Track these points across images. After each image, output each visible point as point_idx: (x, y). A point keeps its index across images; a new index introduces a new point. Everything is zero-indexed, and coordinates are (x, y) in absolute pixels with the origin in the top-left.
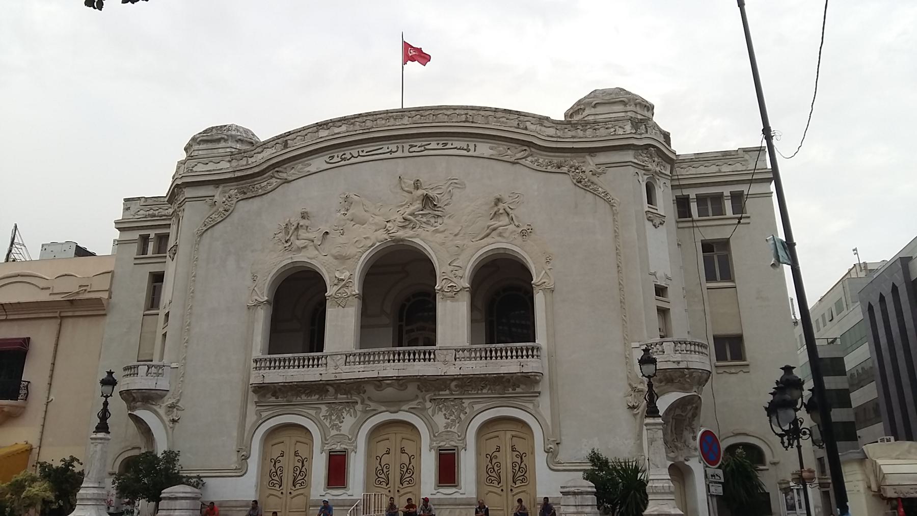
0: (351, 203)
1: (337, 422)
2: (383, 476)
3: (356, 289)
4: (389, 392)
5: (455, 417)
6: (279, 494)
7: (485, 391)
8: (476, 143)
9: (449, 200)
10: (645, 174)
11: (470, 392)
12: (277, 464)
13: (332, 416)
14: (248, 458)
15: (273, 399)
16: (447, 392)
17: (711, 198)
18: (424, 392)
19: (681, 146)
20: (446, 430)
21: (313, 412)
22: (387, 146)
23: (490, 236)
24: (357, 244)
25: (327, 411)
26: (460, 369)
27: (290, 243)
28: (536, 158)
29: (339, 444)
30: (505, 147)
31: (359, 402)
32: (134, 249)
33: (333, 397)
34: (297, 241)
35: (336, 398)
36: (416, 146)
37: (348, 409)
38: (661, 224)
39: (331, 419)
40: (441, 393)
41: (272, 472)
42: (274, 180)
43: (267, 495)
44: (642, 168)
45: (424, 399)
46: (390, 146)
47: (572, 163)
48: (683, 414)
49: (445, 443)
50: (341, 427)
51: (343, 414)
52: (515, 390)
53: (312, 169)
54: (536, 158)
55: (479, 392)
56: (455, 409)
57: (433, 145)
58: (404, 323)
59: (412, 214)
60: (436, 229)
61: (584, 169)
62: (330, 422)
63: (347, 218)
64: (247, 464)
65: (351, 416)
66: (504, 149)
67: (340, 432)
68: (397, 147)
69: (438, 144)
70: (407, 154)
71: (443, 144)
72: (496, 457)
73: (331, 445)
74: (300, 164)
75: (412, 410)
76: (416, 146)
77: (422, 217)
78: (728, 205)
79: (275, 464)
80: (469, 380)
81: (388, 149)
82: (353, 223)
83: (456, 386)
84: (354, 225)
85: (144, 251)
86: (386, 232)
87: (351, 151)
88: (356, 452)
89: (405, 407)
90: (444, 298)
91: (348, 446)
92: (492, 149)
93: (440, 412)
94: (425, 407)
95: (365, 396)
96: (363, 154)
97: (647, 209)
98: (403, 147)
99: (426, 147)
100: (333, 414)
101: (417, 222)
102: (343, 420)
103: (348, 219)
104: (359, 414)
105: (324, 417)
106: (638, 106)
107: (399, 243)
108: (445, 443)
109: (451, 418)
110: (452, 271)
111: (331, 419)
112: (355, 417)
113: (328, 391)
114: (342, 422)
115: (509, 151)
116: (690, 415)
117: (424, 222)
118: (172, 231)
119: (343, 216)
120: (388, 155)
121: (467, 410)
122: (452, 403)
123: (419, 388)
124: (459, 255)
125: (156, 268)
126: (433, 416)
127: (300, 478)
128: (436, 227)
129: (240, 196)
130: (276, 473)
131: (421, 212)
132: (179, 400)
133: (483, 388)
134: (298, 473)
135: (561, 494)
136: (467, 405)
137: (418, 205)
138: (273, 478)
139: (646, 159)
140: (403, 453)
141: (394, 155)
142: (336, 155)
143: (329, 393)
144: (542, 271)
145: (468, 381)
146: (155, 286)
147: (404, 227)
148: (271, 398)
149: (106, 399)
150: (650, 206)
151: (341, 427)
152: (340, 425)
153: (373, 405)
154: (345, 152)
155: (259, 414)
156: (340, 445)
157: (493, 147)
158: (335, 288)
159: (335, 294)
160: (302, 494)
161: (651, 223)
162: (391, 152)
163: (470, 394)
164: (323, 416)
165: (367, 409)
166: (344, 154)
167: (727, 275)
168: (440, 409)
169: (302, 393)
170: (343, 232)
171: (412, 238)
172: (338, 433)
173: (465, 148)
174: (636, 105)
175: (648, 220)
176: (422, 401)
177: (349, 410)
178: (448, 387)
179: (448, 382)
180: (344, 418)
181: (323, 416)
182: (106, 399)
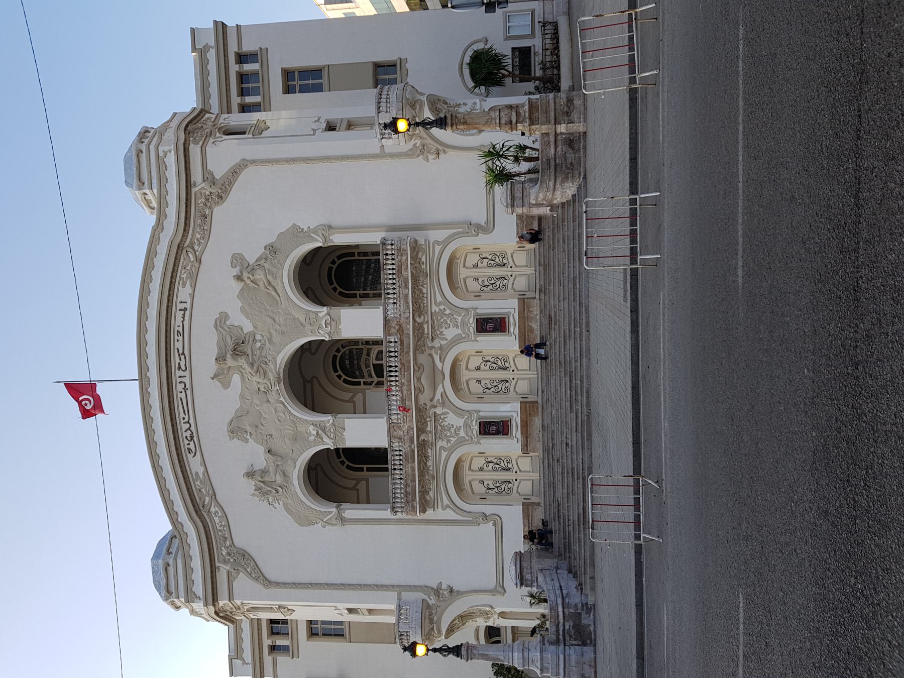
0: (239, 428)
1: (452, 430)
2: (500, 386)
3: (328, 419)
4: (423, 381)
6: (516, 483)
7: (424, 291)
8: (179, 301)
9: (238, 329)
10: (215, 135)
11: (425, 305)
12: (490, 487)
14: (485, 514)
15: (431, 493)
16: (425, 326)
17: (242, 83)
18: (426, 348)
19: (188, 102)
21: (444, 454)
22: (179, 393)
23: (276, 288)
24: (282, 421)
25: (443, 440)
27: (279, 488)
28: (196, 241)
29: (472, 427)
30: (183, 271)
31: (433, 410)
32: (282, 659)
34: (277, 482)
35: (431, 432)
36: (179, 363)
38: (265, 123)
39: (450, 437)
40: (426, 332)
41: (497, 491)
42: (213, 509)
43: (518, 495)
44: (208, 138)
45: (433, 347)
46: (179, 391)
47: (202, 205)
48: (444, 111)
49: (471, 328)
53: (201, 470)
54: (196, 241)
55: (425, 296)
56: (440, 319)
57: (179, 345)
58: (362, 380)
59: (252, 365)
60: (268, 339)
61: (207, 193)
62: (453, 437)
63: (254, 431)
64: (490, 515)
66: (185, 272)
68: (180, 382)
69: (178, 341)
70: (187, 373)
71: (178, 335)
72: (483, 281)
73: (474, 435)
74: (196, 483)
75: (442, 360)
76: (179, 363)
77: (255, 355)
78: (248, 67)
79: (490, 489)
80: (415, 305)
81: (181, 392)
82: (260, 426)
83: (420, 317)
84: (262, 424)
85: (284, 649)
86: (270, 392)
87: (184, 430)
88: (480, 411)
89: (439, 365)
90: (338, 331)
92: (185, 285)
93: (444, 333)
94: (438, 347)
95: (429, 404)
96: (187, 417)
97: (251, 136)
98: (180, 377)
99: (180, 353)
100: (446, 435)
101: (261, 359)
103: (256, 431)
104: (445, 410)
106: (143, 140)
107: (282, 378)
108: (471, 328)
109: (449, 322)
110: (311, 324)
112: (448, 413)
113: (424, 440)
114: (453, 425)
115: (188, 268)
116: (445, 106)
117: (261, 353)
118: (265, 616)
119: (252, 437)
120: (188, 392)
121: (442, 307)
122: (436, 322)
123: (423, 353)
124: (294, 318)
125: (303, 631)
126: (447, 340)
127: (502, 464)
128: (265, 341)
129: (228, 543)
130: (498, 487)
131: (250, 357)
132: (432, 588)
133: (421, 291)
134: (498, 466)
135: (515, 214)
136: (438, 308)
137: (242, 361)
138: (503, 490)
139: (199, 133)
141: (188, 386)
142: (187, 446)
143: (426, 439)
144: (311, 236)
145: (415, 305)
146: (324, 635)
147: (265, 374)
148: (430, 496)
149: (430, 650)
150: (247, 133)
153: (438, 396)
154: (184, 436)
155: (444, 508)
157: (183, 284)
158: (326, 439)
159: (332, 439)
160: (517, 461)
161: (265, 134)
162: (185, 389)
163: (427, 306)
165: (441, 402)
166: (186, 437)
167: (317, 72)
168: (441, 333)
170: (269, 435)
171: (276, 365)
172: (462, 428)
173: (183, 312)
174: (142, 142)
175: (261, 134)
176: (433, 350)
178: (421, 325)
179: (416, 325)
182: (430, 650)
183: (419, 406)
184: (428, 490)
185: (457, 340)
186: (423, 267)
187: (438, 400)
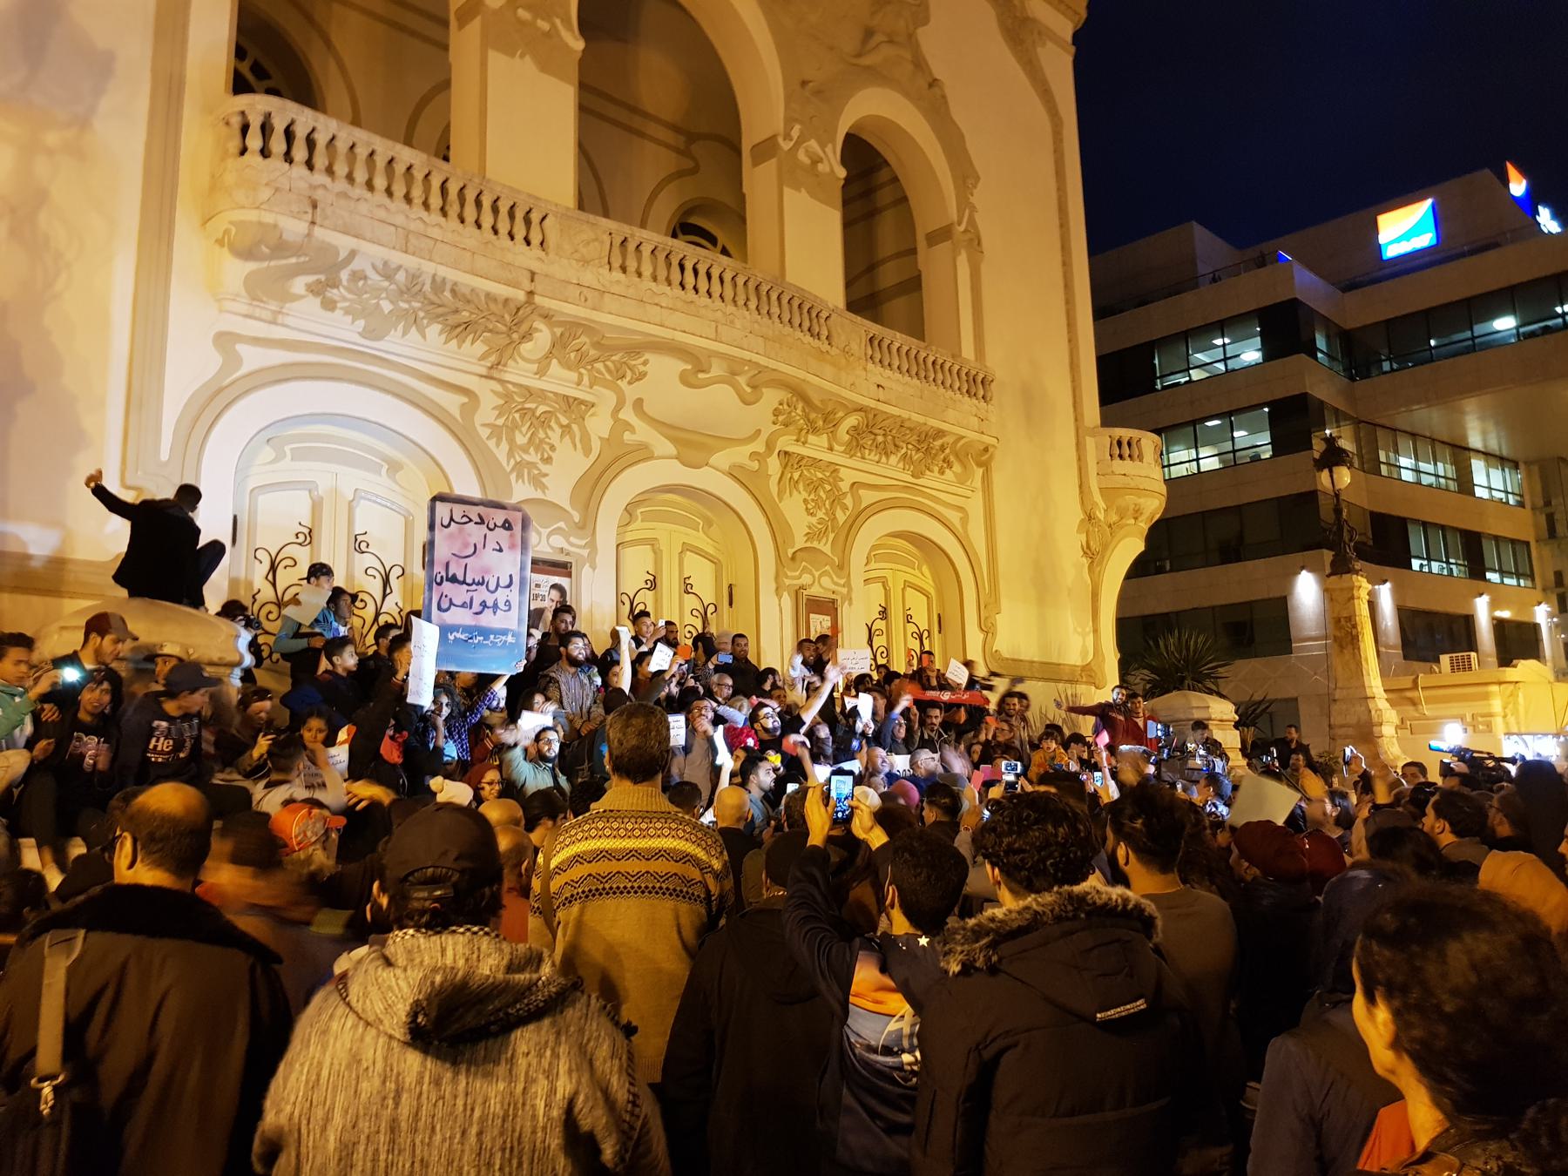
1: (532, 457)
5: (826, 514)
7: (894, 459)
12: (280, 571)
13: (517, 432)
16: (823, 440)
20: (808, 545)
25: (501, 412)
26: (878, 386)
33: (535, 367)
37: (564, 421)
39: (511, 441)
40: (812, 438)
50: (546, 475)
51: (550, 433)
52: (942, 472)
62: (510, 454)
65: (575, 446)
67: (544, 492)
91: (572, 545)
95: (631, 392)
102: (553, 455)
104: (596, 446)
105: (488, 431)
109: (821, 514)
111: (511, 441)
114: (548, 460)
121: (848, 501)
140: (689, 593)
148: (300, 297)
151: (546, 475)
152: (544, 468)
153: (642, 432)
156: (549, 536)
164: (484, 425)
169: (436, 318)
172: (538, 495)
177: (568, 426)
180: (553, 448)
181: (484, 425)
183: (647, 356)
184: (333, 293)
185: (778, 529)
186: (936, 469)
187: (631, 429)
